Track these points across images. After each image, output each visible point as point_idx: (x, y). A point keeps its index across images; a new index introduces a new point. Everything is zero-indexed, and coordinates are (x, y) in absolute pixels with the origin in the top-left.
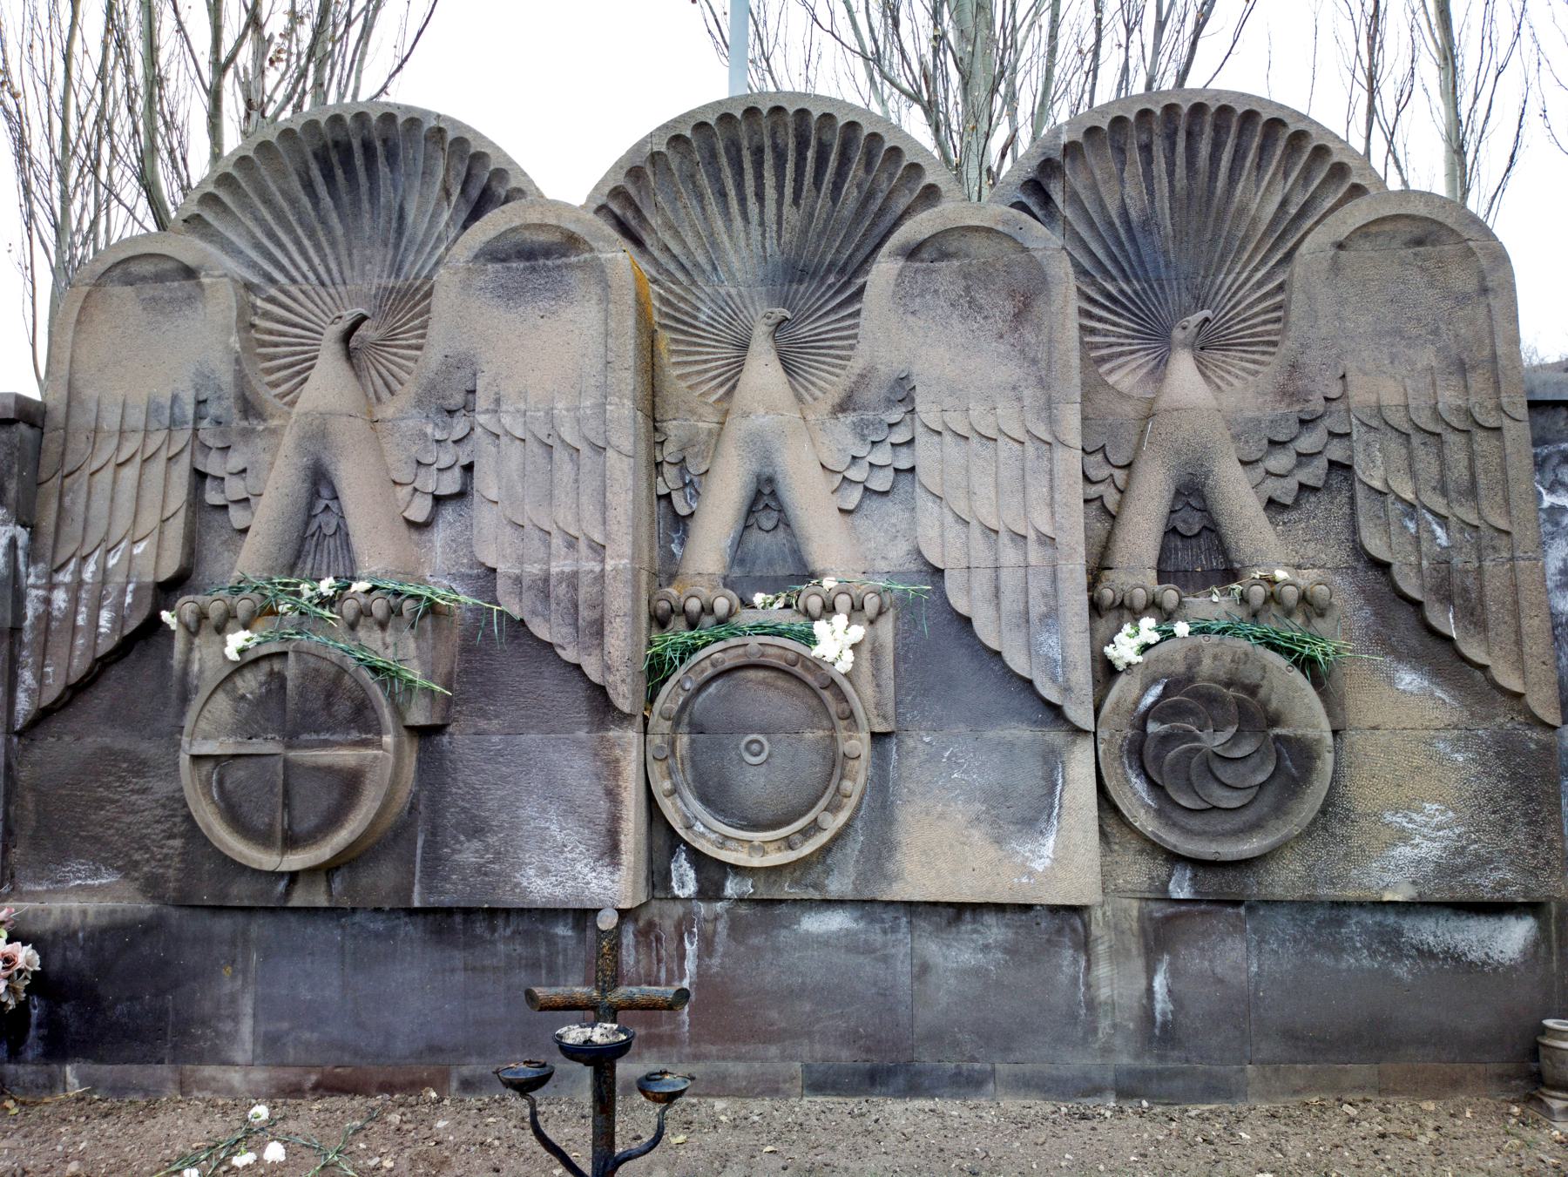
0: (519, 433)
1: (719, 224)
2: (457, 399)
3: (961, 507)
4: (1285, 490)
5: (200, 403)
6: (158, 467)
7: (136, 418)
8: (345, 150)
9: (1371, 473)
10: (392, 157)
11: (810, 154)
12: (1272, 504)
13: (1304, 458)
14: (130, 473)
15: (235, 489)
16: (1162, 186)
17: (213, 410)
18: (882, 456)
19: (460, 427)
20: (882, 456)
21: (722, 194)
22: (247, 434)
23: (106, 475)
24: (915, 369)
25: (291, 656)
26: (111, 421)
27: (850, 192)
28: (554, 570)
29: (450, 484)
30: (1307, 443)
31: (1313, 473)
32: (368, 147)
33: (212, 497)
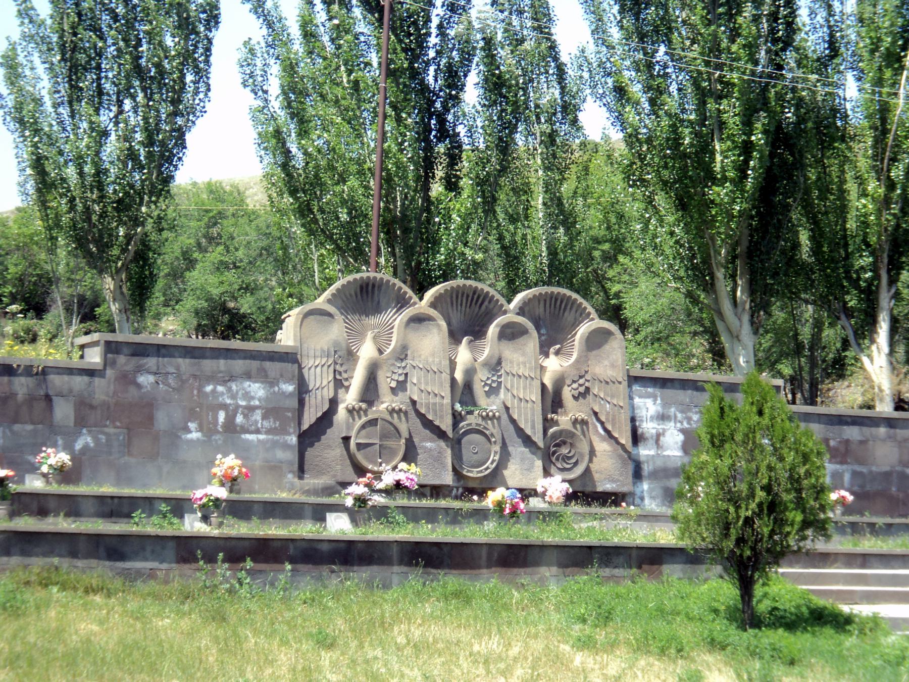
0: (421, 366)
1: (450, 311)
2: (403, 356)
3: (515, 393)
4: (576, 393)
5: (335, 352)
6: (325, 367)
7: (318, 353)
8: (367, 285)
9: (596, 391)
10: (380, 286)
11: (476, 297)
12: (573, 396)
13: (581, 385)
14: (319, 369)
15: (345, 375)
16: (548, 311)
17: (339, 353)
18: (495, 378)
19: (403, 364)
20: (495, 378)
21: (452, 304)
22: (348, 360)
23: (313, 369)
24: (503, 356)
25: (379, 421)
26: (312, 353)
27: (484, 307)
28: (431, 401)
29: (402, 378)
30: (581, 381)
31: (582, 389)
32: (374, 286)
33: (338, 377)
